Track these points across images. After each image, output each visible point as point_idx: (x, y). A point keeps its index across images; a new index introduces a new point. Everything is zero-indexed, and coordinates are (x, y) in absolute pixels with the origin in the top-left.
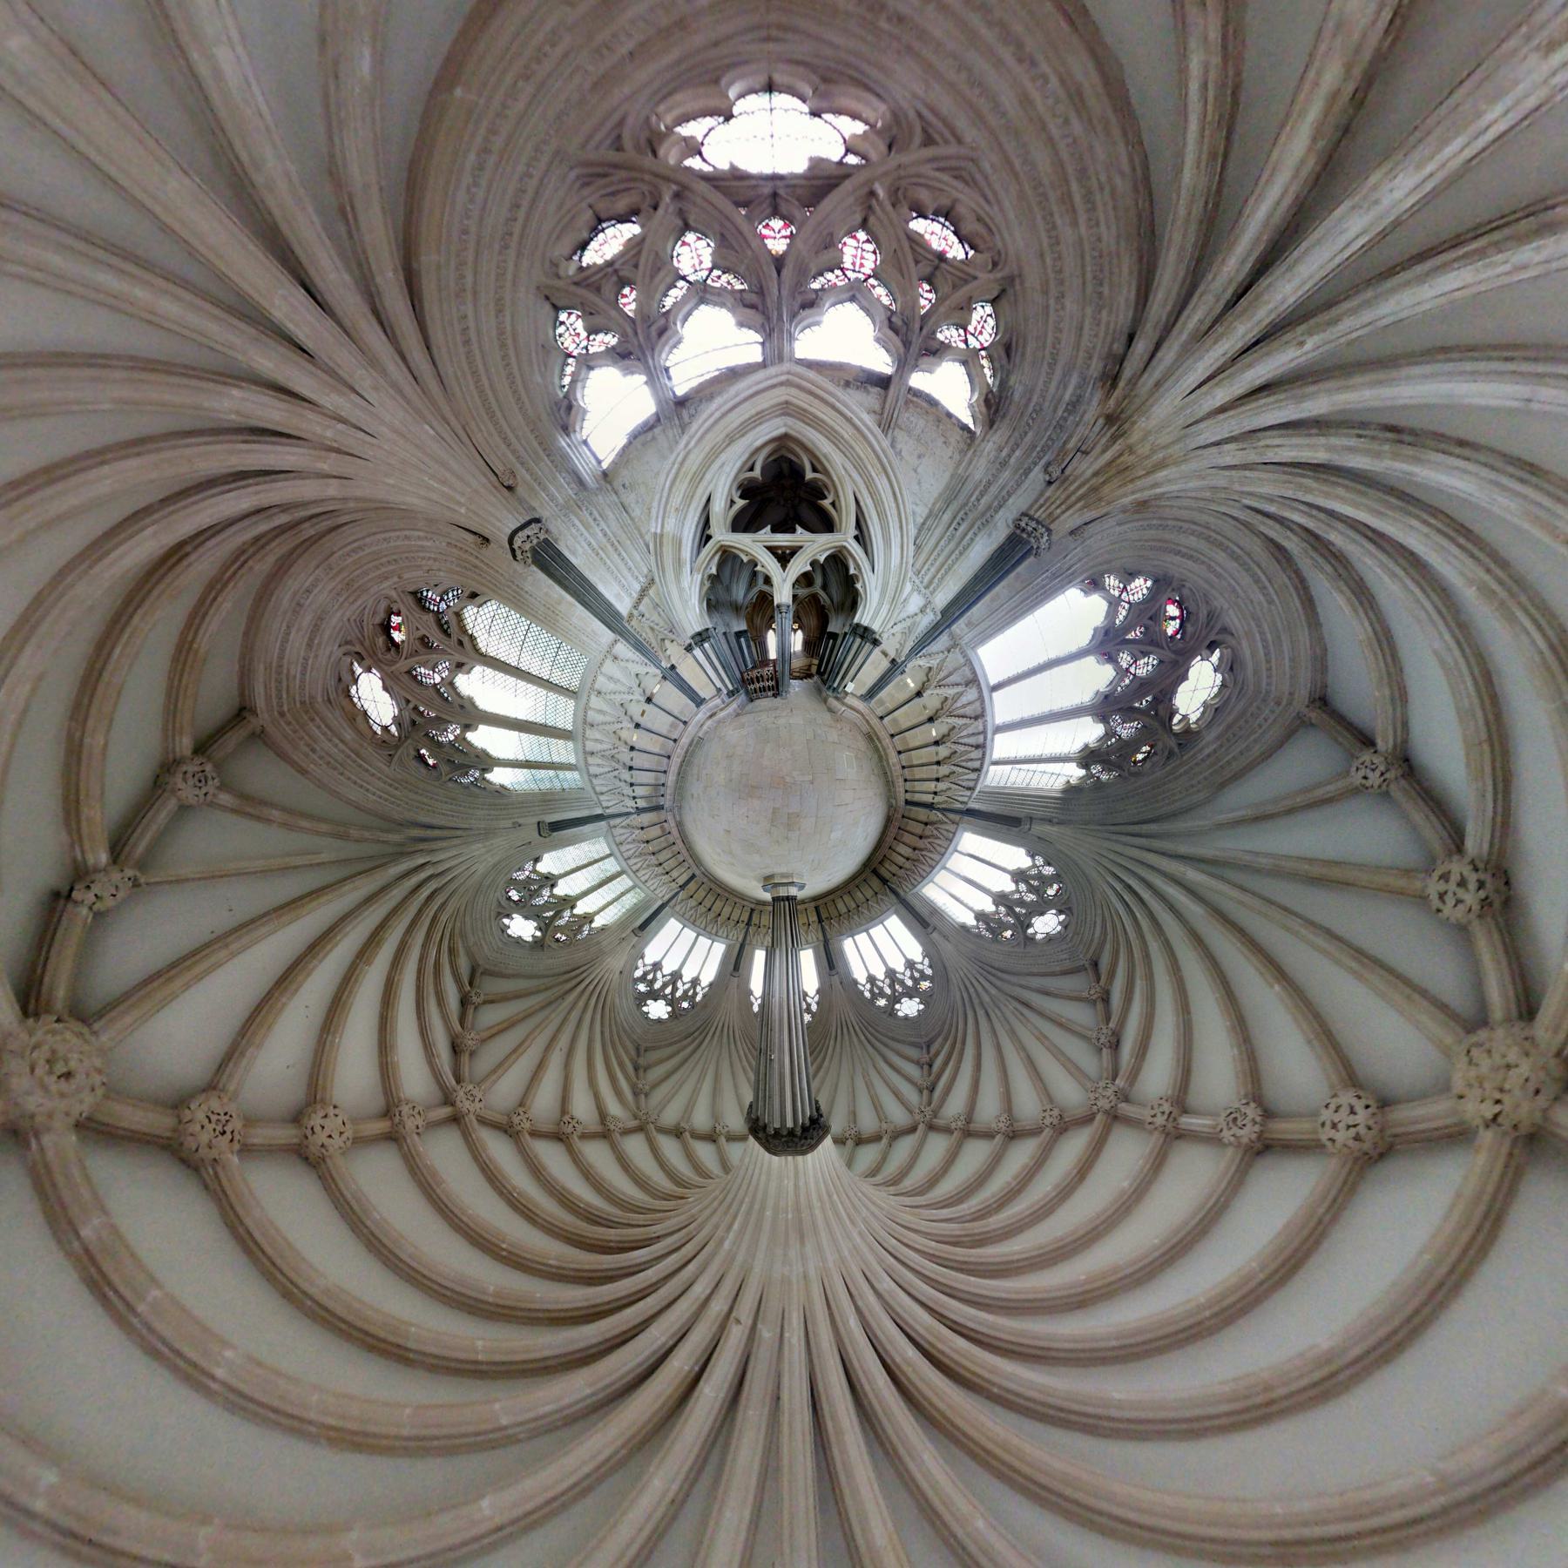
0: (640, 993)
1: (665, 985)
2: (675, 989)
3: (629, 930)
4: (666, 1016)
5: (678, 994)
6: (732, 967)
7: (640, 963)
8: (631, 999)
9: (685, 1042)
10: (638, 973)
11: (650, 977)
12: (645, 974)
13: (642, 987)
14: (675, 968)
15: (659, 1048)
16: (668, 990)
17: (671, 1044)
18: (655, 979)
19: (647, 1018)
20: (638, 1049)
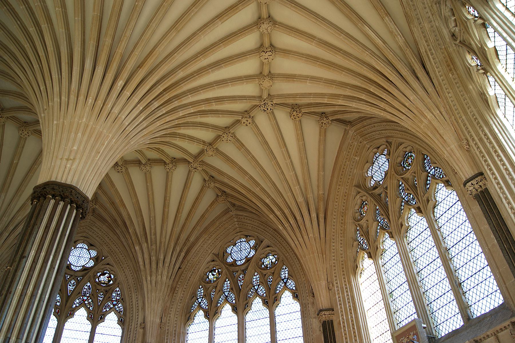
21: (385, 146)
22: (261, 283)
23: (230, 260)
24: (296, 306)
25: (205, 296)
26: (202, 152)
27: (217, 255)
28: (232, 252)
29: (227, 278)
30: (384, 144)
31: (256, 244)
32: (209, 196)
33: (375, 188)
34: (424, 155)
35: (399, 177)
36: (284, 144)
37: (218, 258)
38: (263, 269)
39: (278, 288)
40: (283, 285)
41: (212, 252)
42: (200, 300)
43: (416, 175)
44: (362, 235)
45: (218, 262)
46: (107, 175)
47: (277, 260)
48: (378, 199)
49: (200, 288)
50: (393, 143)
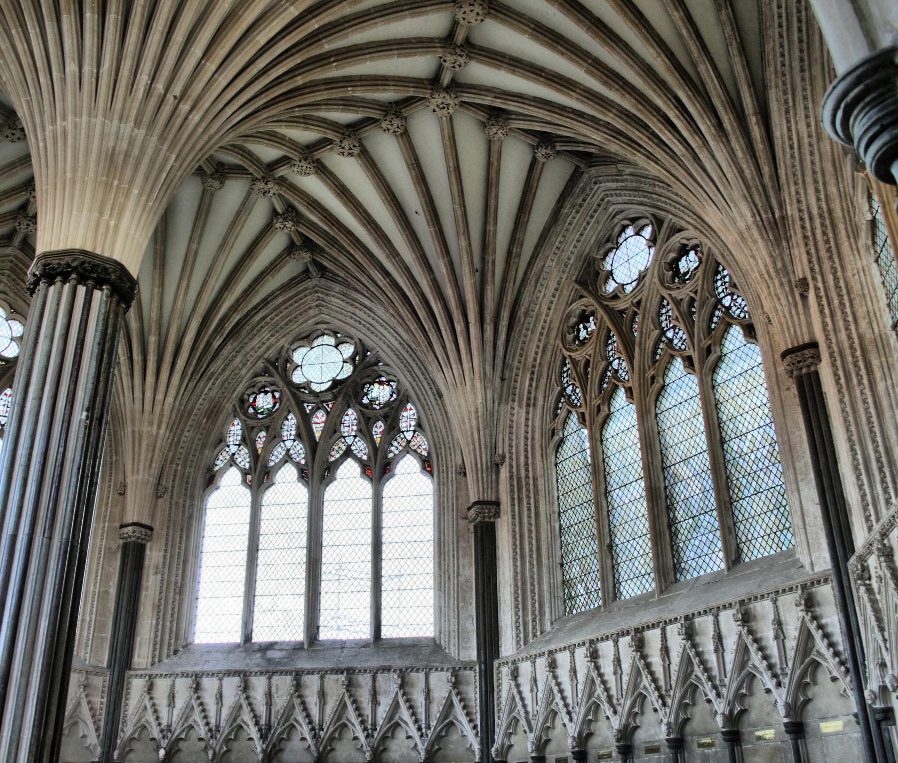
0: (376, 379)
1: (333, 429)
2: (304, 433)
3: (505, 499)
4: (298, 356)
5: (291, 424)
6: (153, 556)
7: (422, 443)
8: (386, 355)
9: (237, 317)
10: (408, 418)
11: (379, 428)
12: (393, 429)
13: (380, 393)
14: (331, 492)
15: (284, 288)
16: (319, 420)
17: (265, 302)
18: (364, 430)
19: (335, 333)
20: (322, 269)
21: (647, 221)
22: (359, 434)
23: (297, 378)
24: (426, 485)
25: (244, 440)
26: (284, 160)
27: (272, 363)
28: (304, 363)
29: (289, 412)
30: (647, 218)
31: (356, 353)
32: (276, 244)
33: (615, 297)
34: (718, 264)
35: (665, 293)
36: (456, 171)
37: (276, 368)
38: (366, 406)
39: (393, 448)
40: (404, 444)
41: (266, 356)
42: (233, 449)
43: (697, 298)
44: (574, 380)
45: (277, 379)
46: (23, 136)
47: (395, 391)
48: (616, 316)
49: (233, 425)
50: (665, 225)
